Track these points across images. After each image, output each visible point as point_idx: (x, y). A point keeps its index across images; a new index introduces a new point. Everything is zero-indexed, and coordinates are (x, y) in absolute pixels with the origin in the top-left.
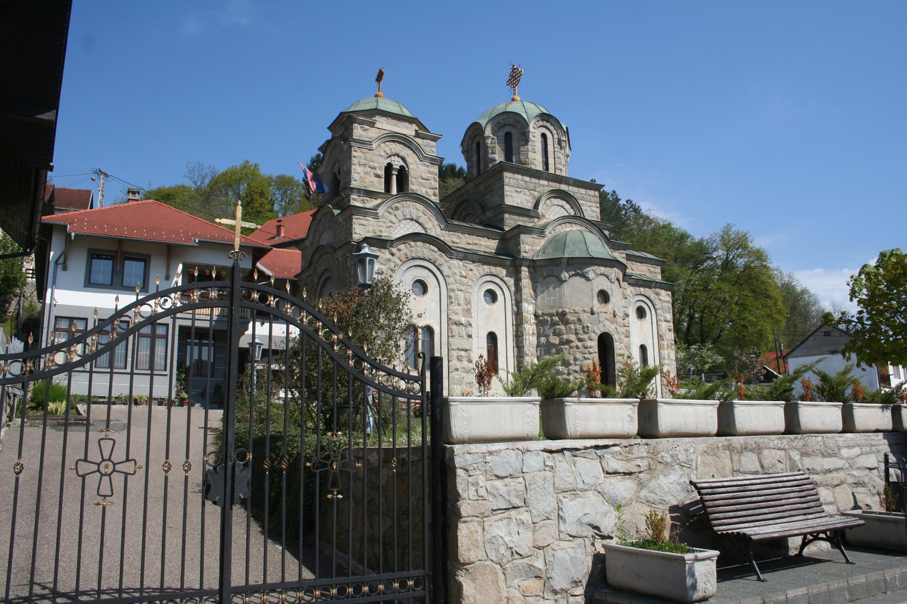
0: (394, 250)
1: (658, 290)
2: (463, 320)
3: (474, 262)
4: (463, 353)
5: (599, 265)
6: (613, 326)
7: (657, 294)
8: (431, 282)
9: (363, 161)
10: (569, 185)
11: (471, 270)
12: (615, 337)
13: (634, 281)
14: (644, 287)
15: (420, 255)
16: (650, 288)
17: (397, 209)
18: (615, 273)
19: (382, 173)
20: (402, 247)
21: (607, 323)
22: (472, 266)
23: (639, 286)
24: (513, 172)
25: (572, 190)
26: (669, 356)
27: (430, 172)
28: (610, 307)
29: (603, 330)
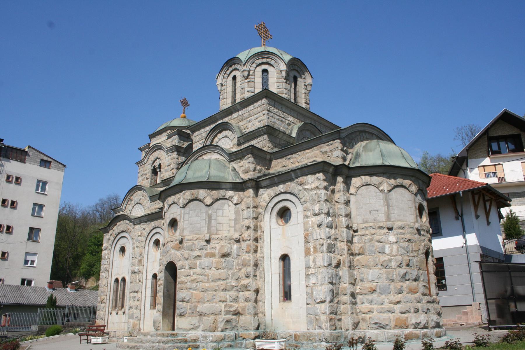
1: (301, 179)
3: (146, 222)
4: (135, 294)
6: (179, 253)
7: (301, 184)
9: (142, 173)
11: (144, 229)
14: (283, 182)
15: (121, 230)
16: (291, 180)
17: (132, 200)
19: (149, 175)
21: (173, 251)
22: (144, 227)
23: (277, 184)
24: (199, 130)
26: (314, 262)
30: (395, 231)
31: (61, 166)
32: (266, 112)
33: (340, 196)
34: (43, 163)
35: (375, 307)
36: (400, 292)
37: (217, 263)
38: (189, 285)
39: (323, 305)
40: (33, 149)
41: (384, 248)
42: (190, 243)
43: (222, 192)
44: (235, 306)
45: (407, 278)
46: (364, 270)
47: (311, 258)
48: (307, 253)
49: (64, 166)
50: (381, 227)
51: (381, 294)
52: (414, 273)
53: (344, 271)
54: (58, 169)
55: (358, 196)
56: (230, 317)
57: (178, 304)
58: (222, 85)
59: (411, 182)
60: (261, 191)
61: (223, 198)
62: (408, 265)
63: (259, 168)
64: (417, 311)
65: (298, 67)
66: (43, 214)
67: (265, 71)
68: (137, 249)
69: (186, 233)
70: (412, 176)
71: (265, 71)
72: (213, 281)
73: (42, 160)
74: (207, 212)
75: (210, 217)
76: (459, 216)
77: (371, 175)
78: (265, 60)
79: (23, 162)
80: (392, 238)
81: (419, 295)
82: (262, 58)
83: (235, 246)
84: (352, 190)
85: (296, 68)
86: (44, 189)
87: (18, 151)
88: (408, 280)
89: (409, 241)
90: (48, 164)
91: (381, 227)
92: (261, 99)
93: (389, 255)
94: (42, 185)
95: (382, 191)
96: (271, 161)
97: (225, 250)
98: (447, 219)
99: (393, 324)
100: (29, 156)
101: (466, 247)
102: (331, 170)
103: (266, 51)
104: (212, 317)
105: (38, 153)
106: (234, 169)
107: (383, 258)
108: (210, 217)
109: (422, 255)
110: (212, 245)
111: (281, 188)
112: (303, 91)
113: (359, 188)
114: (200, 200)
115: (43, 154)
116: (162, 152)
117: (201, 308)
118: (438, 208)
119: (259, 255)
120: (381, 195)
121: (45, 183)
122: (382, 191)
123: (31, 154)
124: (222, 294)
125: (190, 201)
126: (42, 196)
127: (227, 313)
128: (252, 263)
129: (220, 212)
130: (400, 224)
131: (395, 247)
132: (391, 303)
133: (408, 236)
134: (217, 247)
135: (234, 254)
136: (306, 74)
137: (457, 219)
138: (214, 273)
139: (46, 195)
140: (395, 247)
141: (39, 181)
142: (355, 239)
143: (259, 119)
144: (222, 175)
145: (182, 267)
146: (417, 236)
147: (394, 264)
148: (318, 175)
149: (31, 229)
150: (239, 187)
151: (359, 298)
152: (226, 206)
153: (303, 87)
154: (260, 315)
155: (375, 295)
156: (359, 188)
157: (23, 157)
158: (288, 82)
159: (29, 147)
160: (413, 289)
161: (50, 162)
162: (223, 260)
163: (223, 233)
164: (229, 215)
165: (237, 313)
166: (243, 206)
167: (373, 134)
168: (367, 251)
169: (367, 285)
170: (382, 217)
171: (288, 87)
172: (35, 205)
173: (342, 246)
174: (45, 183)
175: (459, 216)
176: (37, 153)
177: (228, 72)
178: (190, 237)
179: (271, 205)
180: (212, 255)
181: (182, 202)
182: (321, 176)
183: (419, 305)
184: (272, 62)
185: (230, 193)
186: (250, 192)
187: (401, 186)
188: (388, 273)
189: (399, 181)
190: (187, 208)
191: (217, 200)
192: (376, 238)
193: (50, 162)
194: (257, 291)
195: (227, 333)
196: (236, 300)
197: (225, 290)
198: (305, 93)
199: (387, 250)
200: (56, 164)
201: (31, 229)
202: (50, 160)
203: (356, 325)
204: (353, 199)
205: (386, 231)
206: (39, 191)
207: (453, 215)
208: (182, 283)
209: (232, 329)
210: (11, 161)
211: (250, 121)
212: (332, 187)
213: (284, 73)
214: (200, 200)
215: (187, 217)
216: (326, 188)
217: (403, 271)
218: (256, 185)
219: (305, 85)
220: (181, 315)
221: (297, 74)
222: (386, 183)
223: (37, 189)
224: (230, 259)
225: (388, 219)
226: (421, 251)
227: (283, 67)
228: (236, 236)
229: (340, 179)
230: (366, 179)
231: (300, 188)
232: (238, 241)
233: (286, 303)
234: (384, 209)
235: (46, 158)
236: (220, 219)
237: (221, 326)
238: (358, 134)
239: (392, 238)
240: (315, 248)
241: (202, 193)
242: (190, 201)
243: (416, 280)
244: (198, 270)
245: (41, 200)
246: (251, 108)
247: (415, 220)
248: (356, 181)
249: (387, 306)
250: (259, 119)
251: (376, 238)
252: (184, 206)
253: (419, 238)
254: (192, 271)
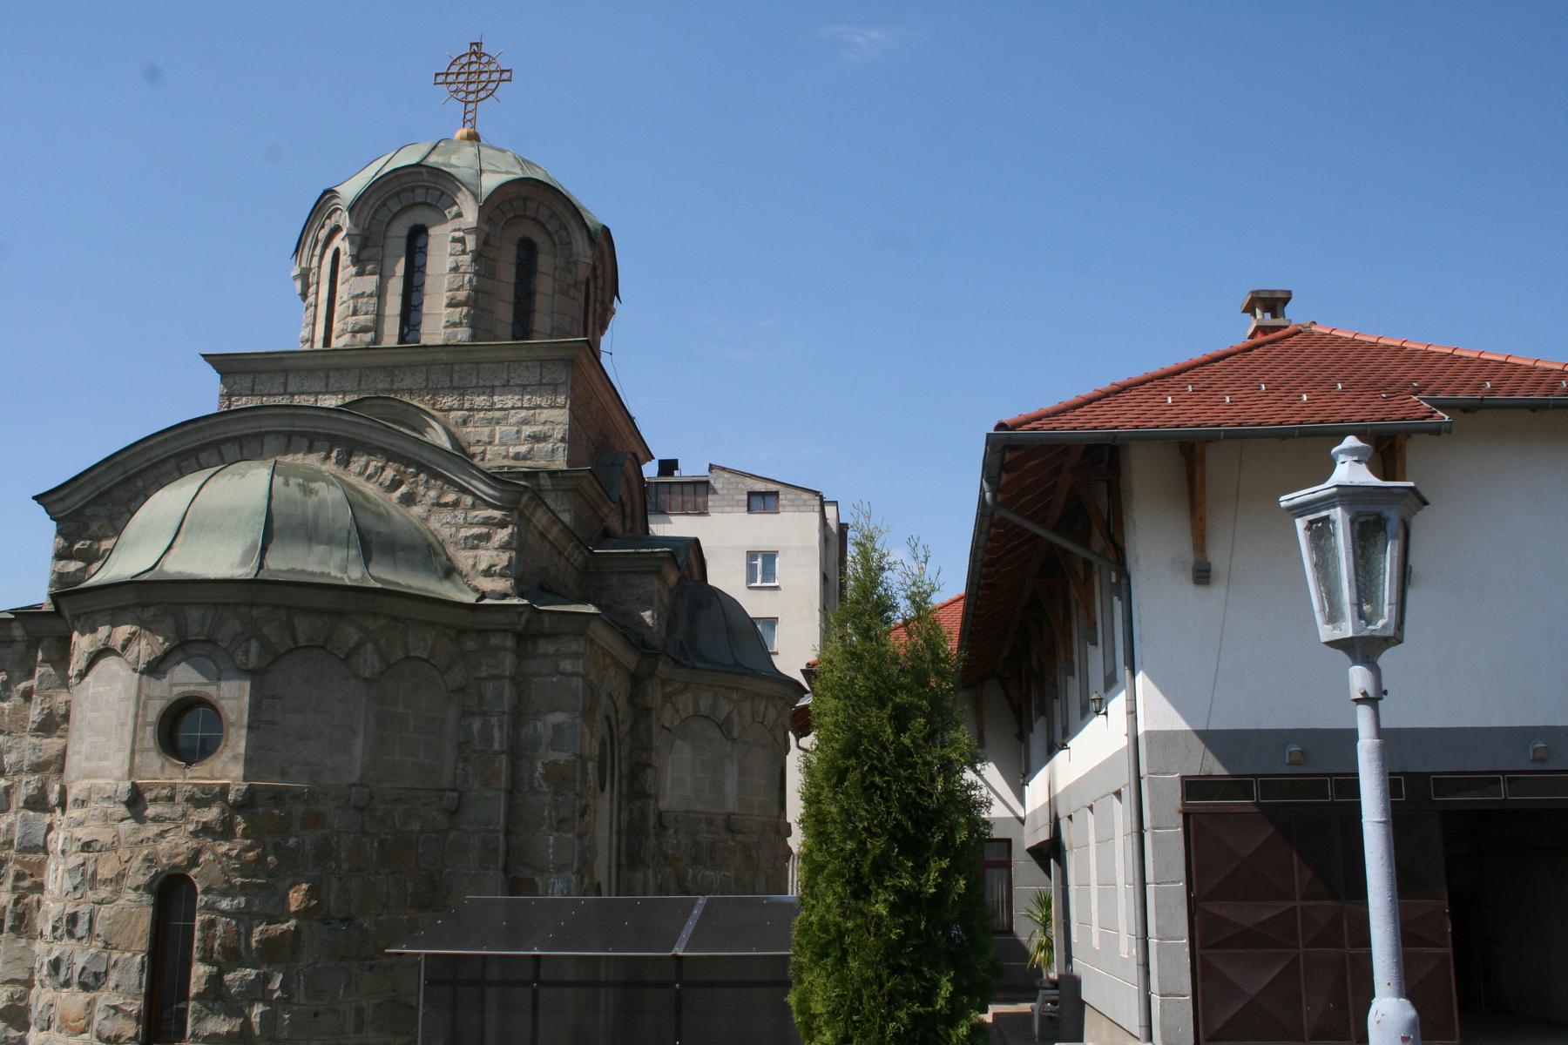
31: (805, 496)
34: (756, 501)
40: (724, 469)
45: (62, 978)
54: (798, 507)
59: (134, 628)
62: (71, 934)
65: (428, 188)
70: (144, 606)
73: (751, 494)
82: (329, 217)
85: (420, 195)
86: (769, 573)
87: (686, 489)
88: (67, 984)
89: (87, 846)
100: (715, 492)
103: (326, 192)
105: (739, 479)
109: (133, 896)
112: (449, 263)
115: (751, 476)
121: (770, 557)
123: (717, 485)
126: (766, 593)
133: (83, 834)
139: (776, 588)
141: (752, 555)
146: (129, 825)
153: (449, 248)
157: (700, 500)
158: (369, 268)
160: (72, 1016)
161: (776, 494)
167: (260, 436)
171: (370, 283)
174: (770, 557)
176: (734, 479)
198: (455, 269)
200: (792, 495)
202: (772, 487)
206: (758, 584)
210: (672, 518)
212: (22, 686)
219: (455, 240)
223: (751, 577)
226: (129, 882)
235: (760, 487)
238: (171, 464)
243: (85, 987)
247: (127, 767)
253: (136, 832)
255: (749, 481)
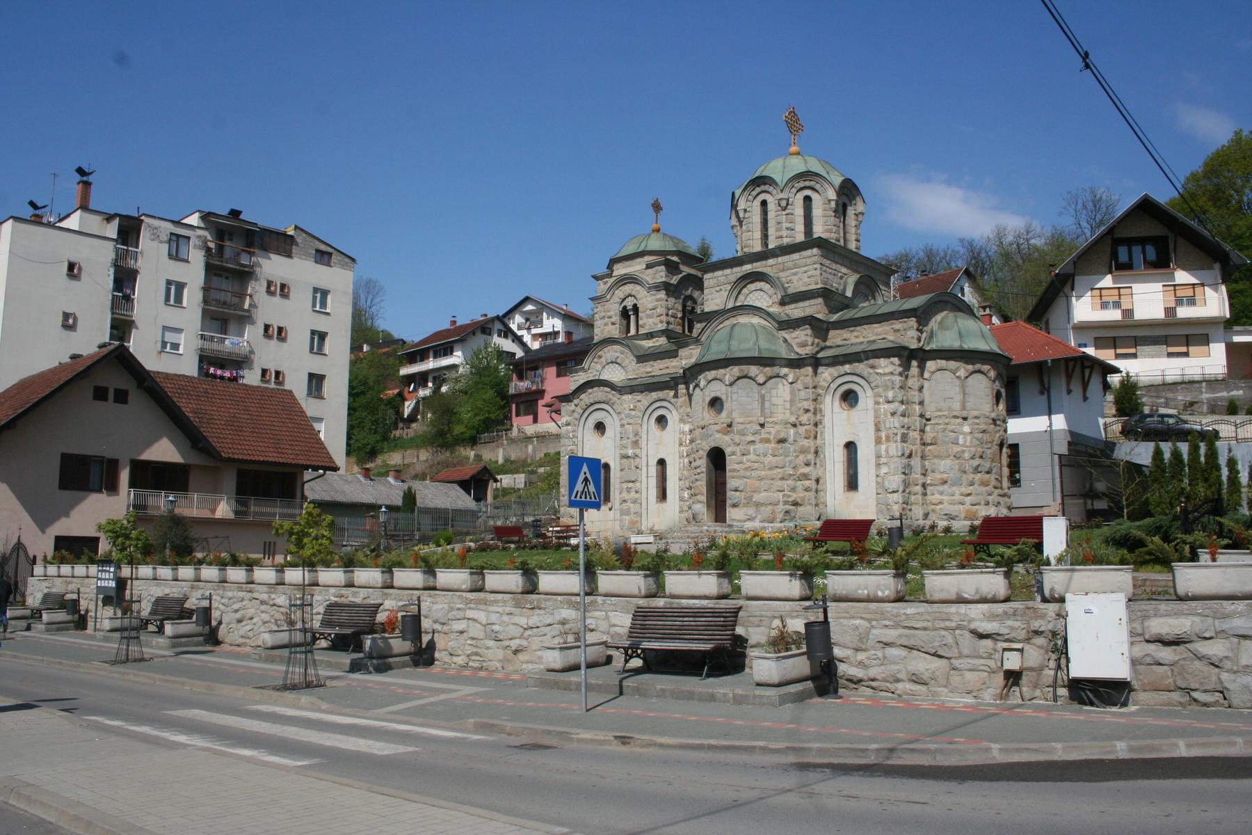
0: (576, 401)
1: (871, 361)
2: (630, 452)
4: (631, 485)
5: (709, 370)
6: (727, 438)
7: (873, 367)
8: (608, 422)
9: (603, 314)
10: (777, 256)
12: (728, 451)
13: (831, 360)
14: (850, 362)
15: (596, 399)
16: (860, 361)
17: (600, 357)
18: (730, 373)
19: (616, 318)
20: (583, 396)
21: (718, 435)
22: (639, 398)
23: (842, 364)
24: (713, 271)
25: (758, 267)
26: (887, 451)
27: (657, 300)
28: (724, 414)
29: (713, 445)
30: (970, 421)
31: (347, 260)
32: (818, 266)
33: (913, 382)
35: (945, 498)
36: (972, 484)
37: (773, 449)
38: (742, 473)
39: (895, 495)
41: (957, 438)
42: (741, 427)
43: (776, 369)
44: (794, 497)
46: (935, 461)
47: (883, 447)
48: (878, 441)
49: (353, 260)
50: (955, 417)
51: (952, 485)
52: (987, 465)
53: (916, 462)
54: (344, 266)
55: (933, 382)
56: (788, 507)
57: (729, 494)
58: (745, 211)
60: (821, 369)
61: (778, 376)
62: (981, 457)
63: (817, 341)
64: (987, 504)
66: (327, 348)
67: (808, 199)
68: (630, 428)
69: (735, 415)
71: (808, 199)
72: (770, 469)
73: (317, 251)
74: (759, 392)
75: (763, 397)
76: (1045, 390)
77: (948, 359)
78: (807, 184)
79: (289, 255)
80: (966, 429)
81: (990, 488)
83: (792, 431)
84: (926, 375)
89: (984, 431)
90: (326, 257)
91: (955, 417)
92: (812, 248)
93: (964, 446)
94: (321, 294)
95: (958, 377)
96: (827, 331)
97: (782, 435)
98: (1028, 392)
99: (963, 515)
101: (1050, 432)
102: (906, 353)
104: (770, 508)
106: (785, 341)
107: (957, 449)
108: (763, 397)
110: (766, 429)
111: (847, 368)
112: (854, 223)
113: (933, 373)
114: (750, 378)
116: (638, 287)
117: (757, 497)
118: (1017, 377)
119: (819, 441)
120: (957, 382)
121: (325, 293)
122: (958, 377)
123: (299, 240)
124: (780, 483)
125: (739, 378)
127: (786, 503)
128: (812, 450)
129: (774, 392)
130: (976, 413)
131: (969, 438)
132: (962, 494)
133: (983, 427)
134: (772, 431)
135: (791, 439)
136: (858, 198)
137: (1042, 393)
138: (769, 459)
140: (969, 438)
142: (928, 428)
143: (810, 273)
144: (773, 347)
145: (733, 453)
147: (967, 455)
148: (892, 359)
149: (312, 376)
150: (796, 364)
151: (929, 489)
152: (780, 386)
154: (821, 506)
155: (946, 487)
156: (933, 373)
159: (296, 228)
161: (330, 254)
162: (780, 446)
163: (779, 417)
164: (783, 393)
165: (795, 504)
166: (799, 385)
168: (939, 442)
169: (939, 476)
170: (957, 406)
172: (313, 332)
173: (915, 435)
174: (325, 293)
175: (1045, 390)
176: (309, 238)
177: (754, 193)
178: (741, 420)
179: (833, 386)
180: (768, 441)
181: (728, 379)
182: (896, 360)
183: (990, 498)
184: (817, 187)
185: (785, 370)
186: (810, 369)
187: (979, 371)
188: (961, 465)
189: (978, 366)
190: (735, 388)
191: (771, 378)
192: (950, 427)
193: (330, 254)
194: (817, 481)
195: (786, 524)
196: (793, 490)
197: (782, 479)
199: (961, 441)
200: (340, 257)
201: (312, 376)
203: (926, 516)
204: (926, 384)
205: (960, 420)
207: (1037, 387)
208: (734, 470)
209: (791, 520)
211: (795, 274)
213: (833, 204)
214: (750, 378)
215: (735, 396)
216: (901, 374)
217: (976, 462)
218: (815, 363)
220: (734, 506)
221: (847, 201)
222: (963, 369)
224: (787, 445)
225: (964, 408)
227: (832, 195)
228: (793, 419)
229: (914, 363)
230: (942, 363)
231: (871, 371)
232: (794, 426)
233: (852, 494)
234: (959, 397)
235: (323, 248)
236: (775, 400)
237: (780, 516)
239: (966, 429)
240: (888, 438)
241: (753, 370)
242: (739, 378)
243: (988, 472)
244: (752, 457)
245: (321, 324)
246: (796, 256)
248: (931, 365)
249: (957, 497)
250: (810, 273)
251: (950, 427)
252: (731, 384)
254: (745, 458)
255: (317, 243)
